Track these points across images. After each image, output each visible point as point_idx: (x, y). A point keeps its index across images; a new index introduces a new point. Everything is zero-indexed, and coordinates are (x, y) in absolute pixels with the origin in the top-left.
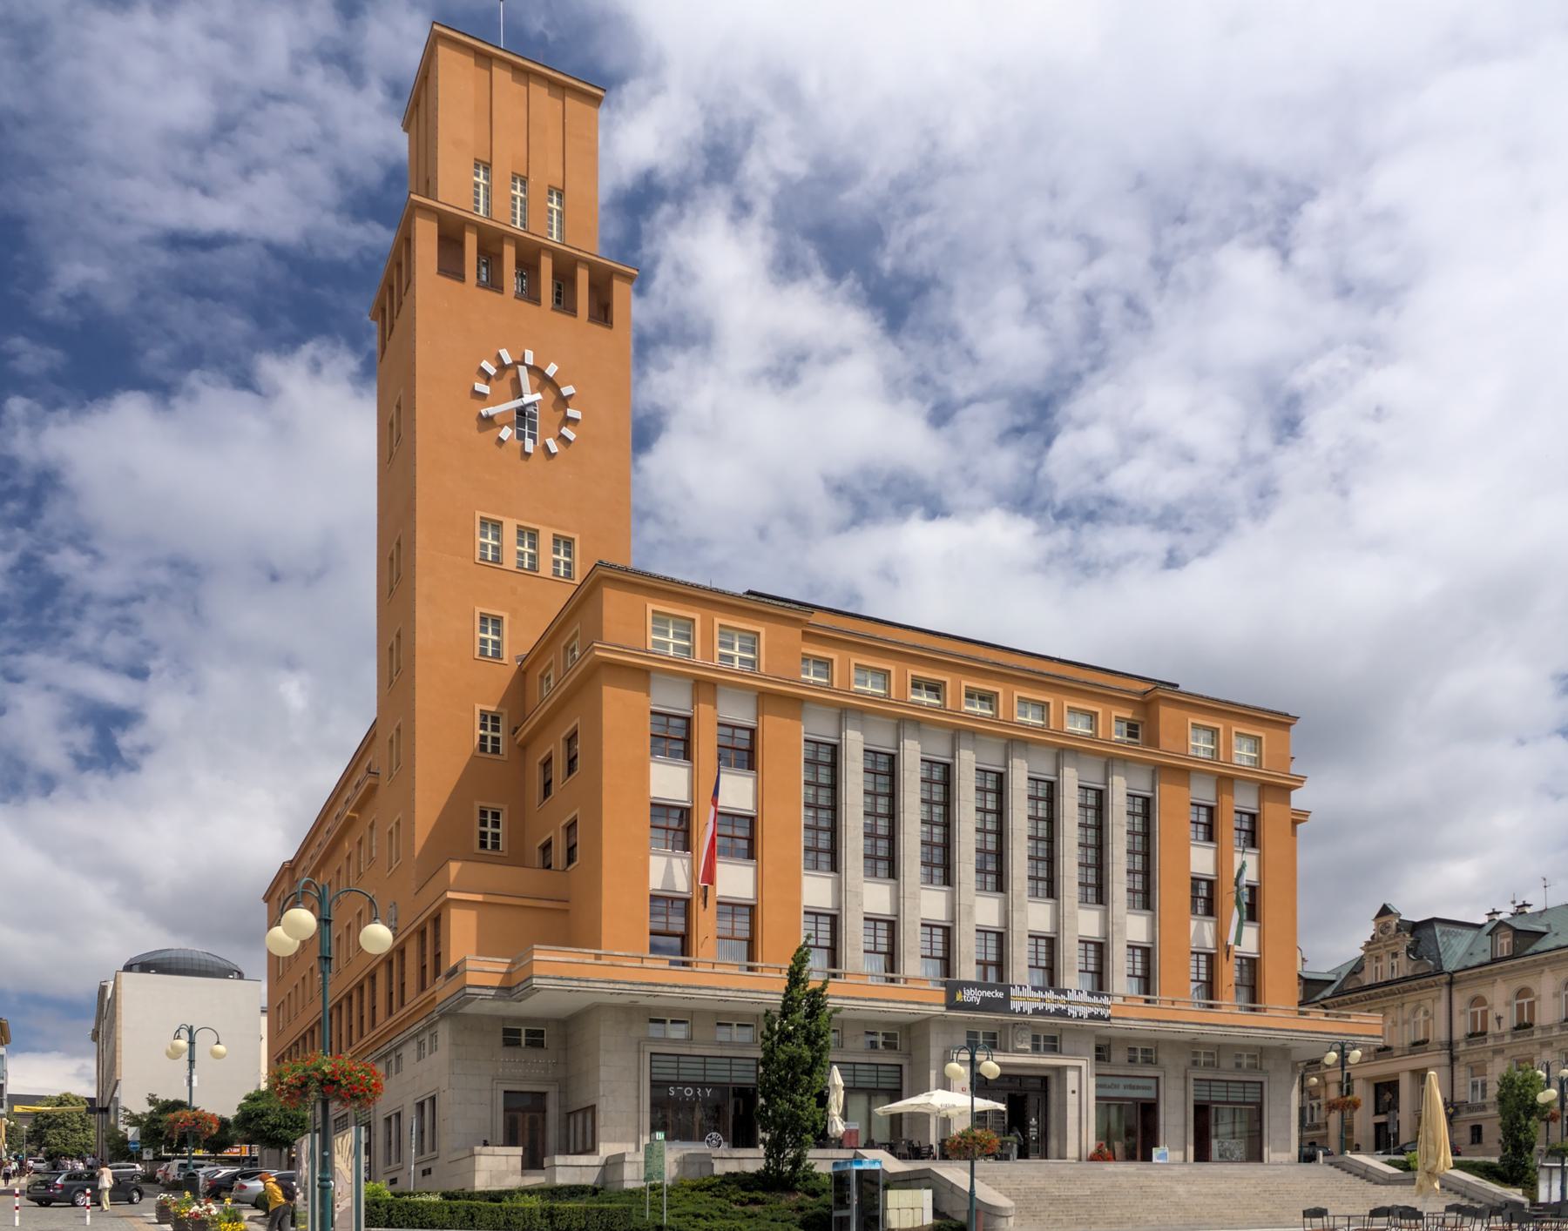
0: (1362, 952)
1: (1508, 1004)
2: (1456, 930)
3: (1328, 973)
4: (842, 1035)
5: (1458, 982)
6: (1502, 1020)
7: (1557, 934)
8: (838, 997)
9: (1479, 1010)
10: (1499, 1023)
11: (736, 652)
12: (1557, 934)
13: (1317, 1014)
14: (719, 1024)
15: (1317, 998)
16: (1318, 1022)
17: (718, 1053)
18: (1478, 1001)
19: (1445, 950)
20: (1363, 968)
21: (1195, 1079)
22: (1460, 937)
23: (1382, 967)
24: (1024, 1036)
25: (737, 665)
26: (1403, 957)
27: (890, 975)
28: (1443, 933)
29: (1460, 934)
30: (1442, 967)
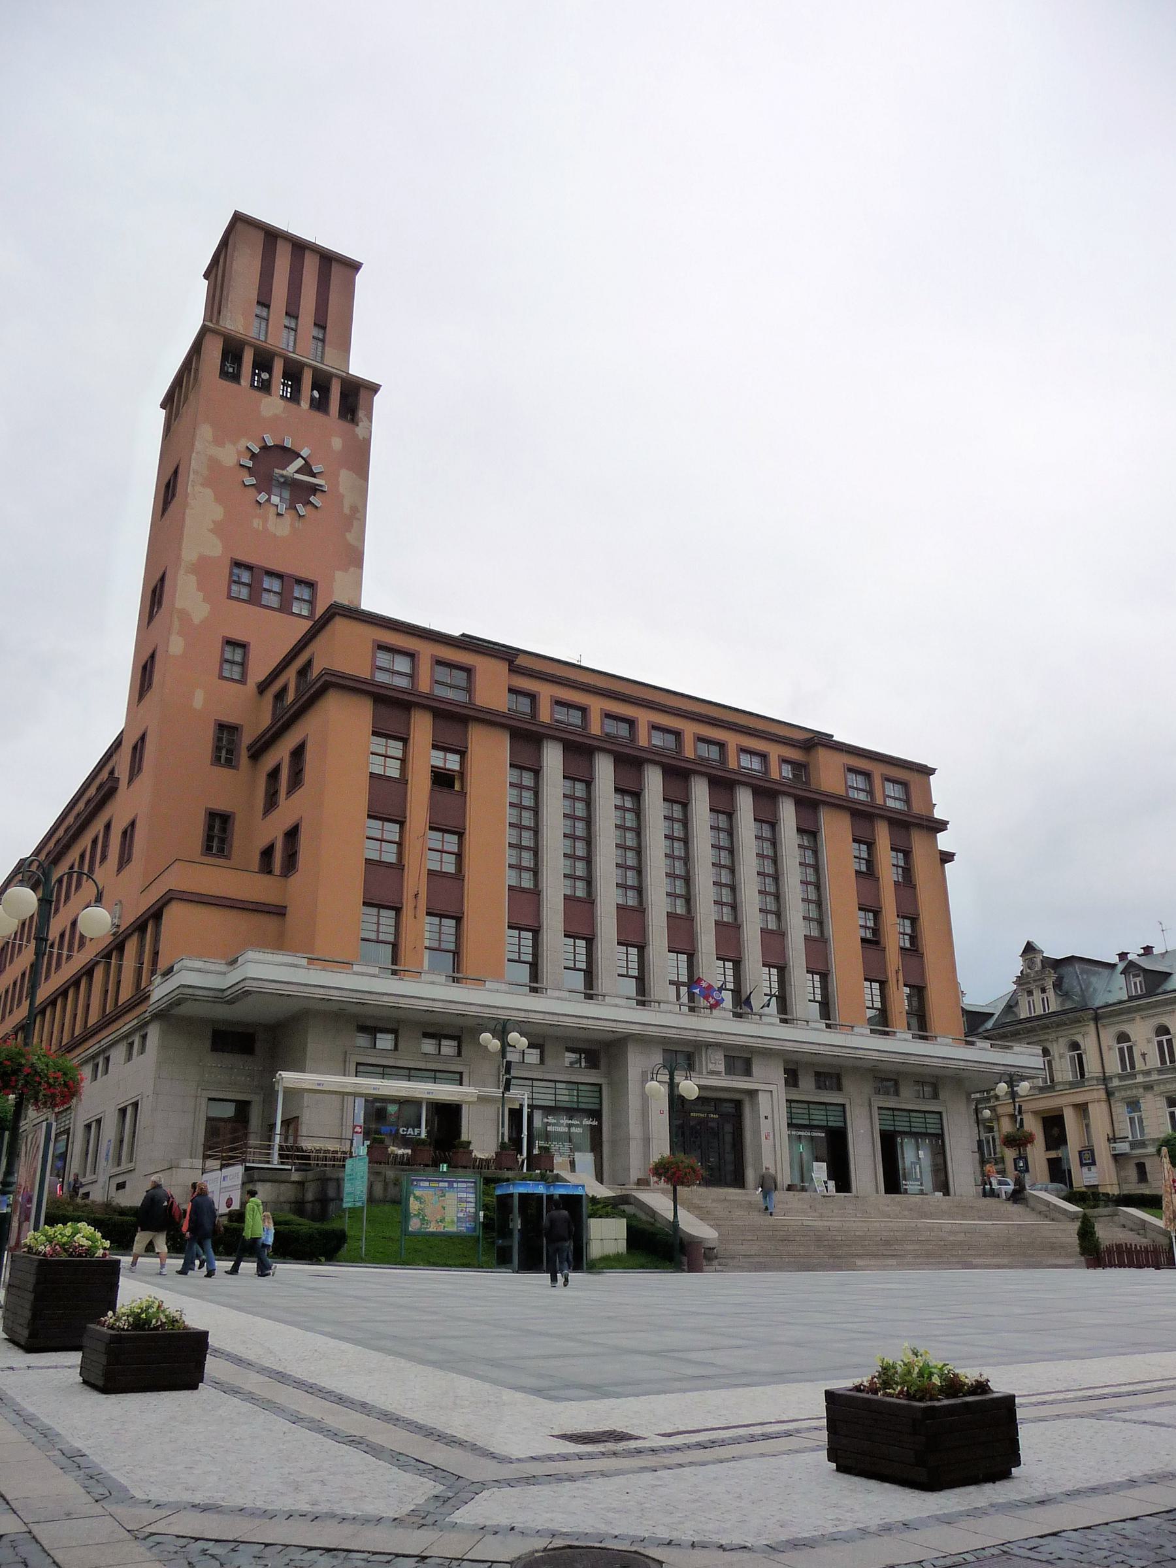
0: (1015, 987)
5: (1101, 1018)
9: (1125, 1045)
10: (1144, 1059)
15: (980, 1030)
16: (983, 1054)
17: (422, 1065)
18: (1123, 1037)
20: (1017, 1003)
26: (1051, 993)
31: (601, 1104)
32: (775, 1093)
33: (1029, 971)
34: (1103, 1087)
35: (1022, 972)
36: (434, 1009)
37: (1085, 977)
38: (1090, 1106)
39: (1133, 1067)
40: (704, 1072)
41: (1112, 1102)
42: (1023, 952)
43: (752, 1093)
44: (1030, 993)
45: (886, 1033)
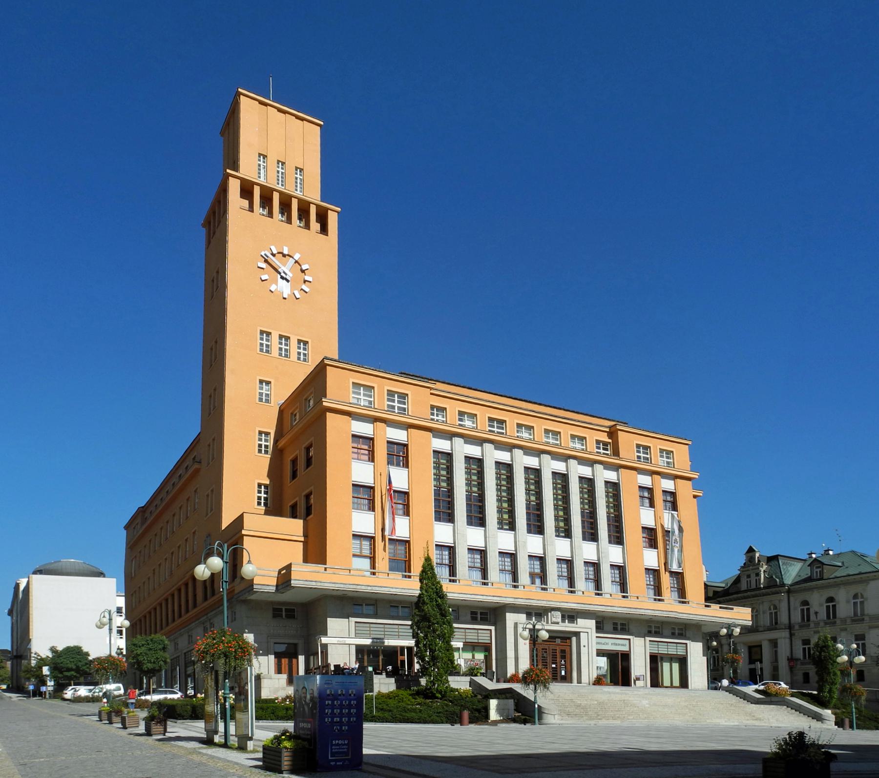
1: (821, 605)
2: (791, 562)
3: (721, 583)
4: (458, 613)
6: (818, 615)
7: (847, 568)
8: (453, 591)
9: (805, 608)
10: (816, 616)
12: (847, 568)
14: (391, 606)
18: (805, 603)
19: (785, 573)
21: (650, 641)
22: (793, 566)
23: (750, 581)
28: (783, 564)
29: (793, 565)
30: (783, 582)
32: (590, 634)
33: (749, 563)
34: (788, 630)
35: (745, 564)
37: (785, 567)
38: (779, 641)
39: (808, 620)
40: (550, 622)
41: (793, 639)
43: (577, 634)
44: (749, 576)
45: (659, 600)
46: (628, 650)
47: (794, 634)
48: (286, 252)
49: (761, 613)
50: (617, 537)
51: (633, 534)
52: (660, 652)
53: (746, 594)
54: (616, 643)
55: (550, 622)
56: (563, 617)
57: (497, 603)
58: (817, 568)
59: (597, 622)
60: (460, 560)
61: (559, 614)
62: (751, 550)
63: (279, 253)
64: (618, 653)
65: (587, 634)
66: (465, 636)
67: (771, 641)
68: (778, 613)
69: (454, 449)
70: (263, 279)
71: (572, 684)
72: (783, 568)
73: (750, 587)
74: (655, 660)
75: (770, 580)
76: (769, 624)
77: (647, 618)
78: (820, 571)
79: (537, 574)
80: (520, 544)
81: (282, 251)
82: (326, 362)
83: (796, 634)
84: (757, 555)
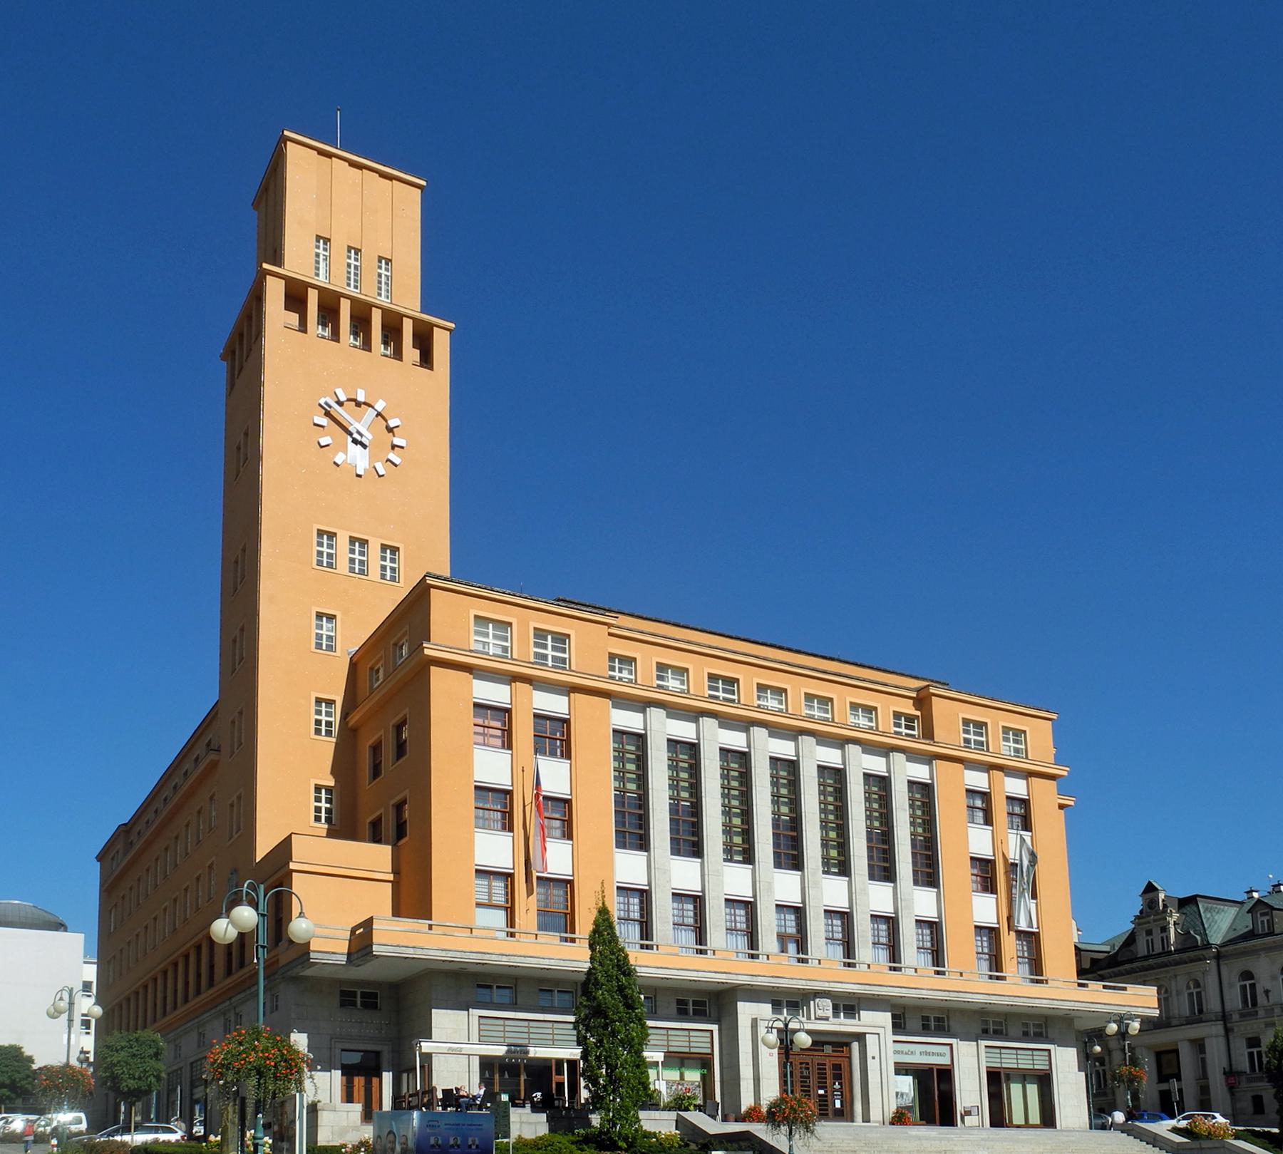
2: (1218, 907)
4: (655, 1002)
5: (1224, 956)
6: (1270, 994)
8: (646, 964)
9: (1247, 983)
11: (549, 652)
13: (1095, 986)
14: (541, 990)
18: (1247, 975)
19: (1210, 925)
21: (986, 1047)
23: (1152, 940)
24: (825, 1004)
25: (550, 663)
27: (699, 947)
28: (1206, 910)
29: (1223, 911)
30: (1208, 941)
31: (713, 1051)
32: (882, 1036)
33: (1148, 910)
34: (1222, 1022)
35: (1141, 912)
36: (550, 967)
37: (1209, 915)
38: (1207, 1042)
39: (1255, 1004)
40: (813, 1017)
42: (1142, 893)
43: (860, 1037)
44: (1149, 933)
45: (998, 978)
46: (949, 1063)
47: (1232, 1030)
48: (361, 398)
49: (1174, 993)
50: (928, 874)
51: (954, 868)
52: (1004, 1066)
53: (1145, 963)
54: (928, 1052)
55: (813, 1017)
56: (836, 1009)
57: (723, 983)
58: (1262, 915)
59: (894, 1017)
60: (660, 912)
61: (827, 1004)
62: (1150, 888)
63: (349, 400)
64: (932, 1069)
65: (877, 1036)
66: (668, 1041)
67: (1192, 1041)
68: (1203, 993)
69: (648, 728)
70: (322, 444)
71: (854, 1124)
72: (1206, 917)
73: (1153, 950)
74: (996, 1079)
75: (1185, 936)
76: (1188, 1014)
77: (976, 1007)
78: (1268, 920)
79: (790, 936)
80: (761, 887)
81: (355, 398)
82: (430, 581)
83: (1236, 1029)
84: (1162, 896)
